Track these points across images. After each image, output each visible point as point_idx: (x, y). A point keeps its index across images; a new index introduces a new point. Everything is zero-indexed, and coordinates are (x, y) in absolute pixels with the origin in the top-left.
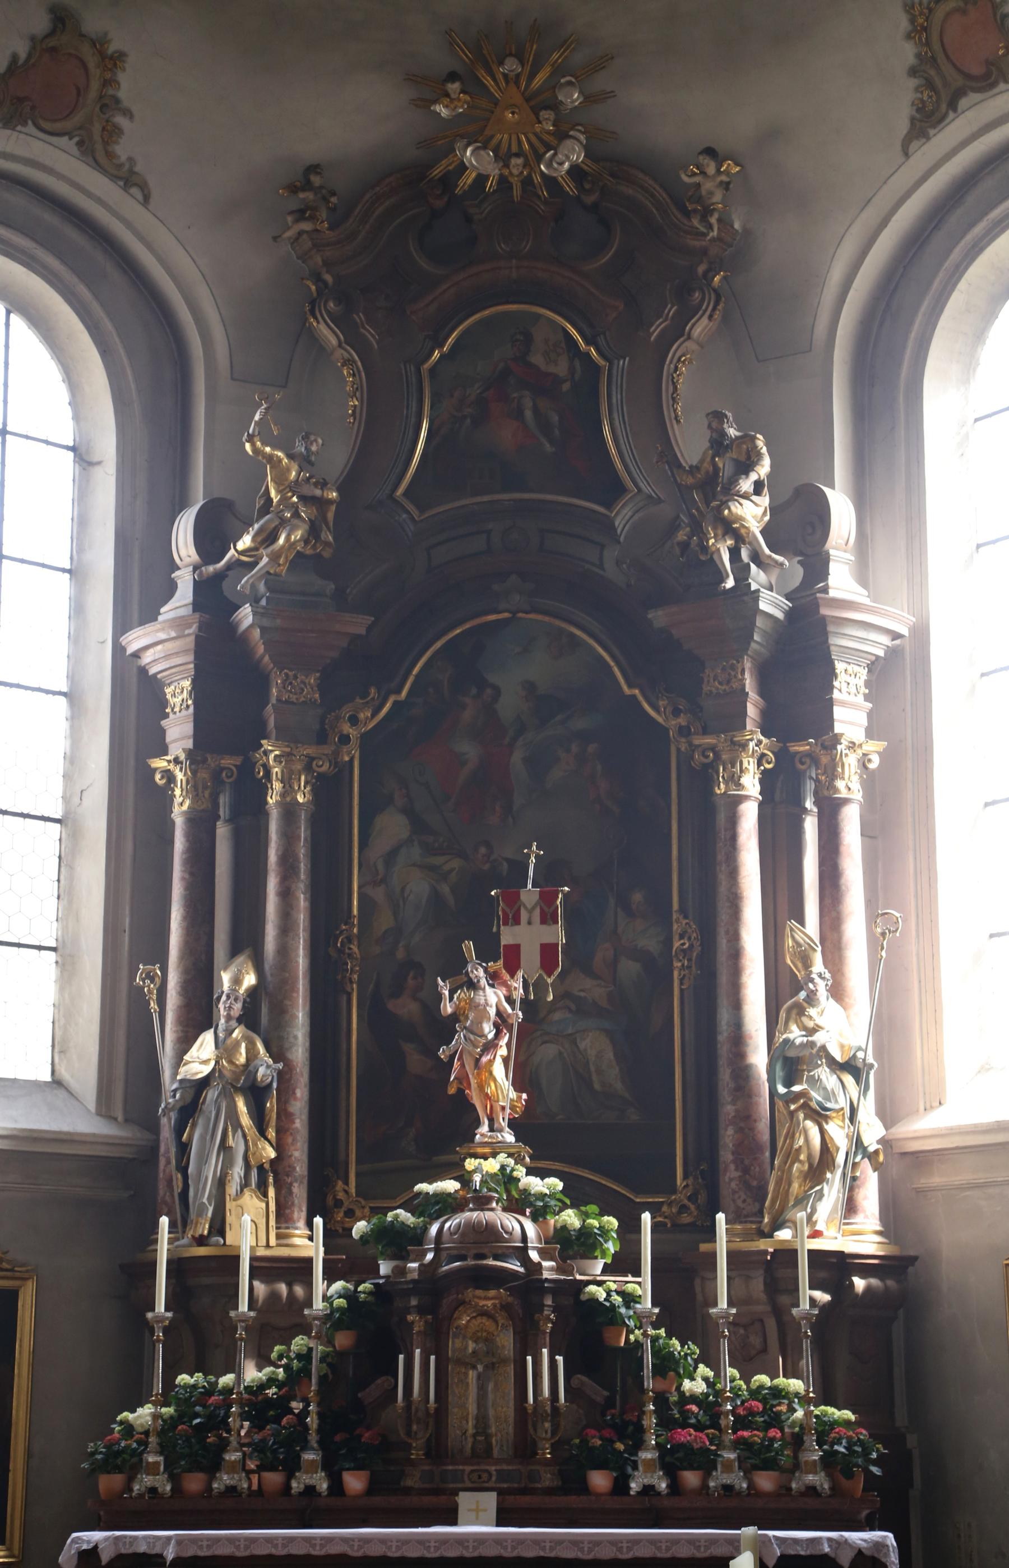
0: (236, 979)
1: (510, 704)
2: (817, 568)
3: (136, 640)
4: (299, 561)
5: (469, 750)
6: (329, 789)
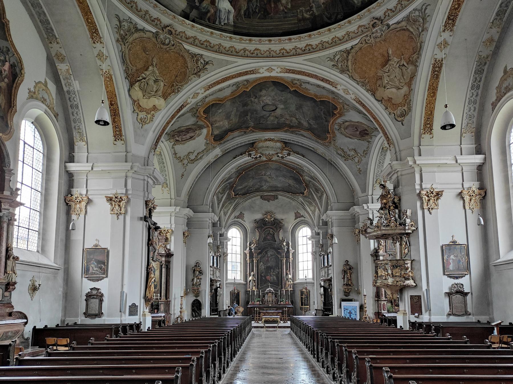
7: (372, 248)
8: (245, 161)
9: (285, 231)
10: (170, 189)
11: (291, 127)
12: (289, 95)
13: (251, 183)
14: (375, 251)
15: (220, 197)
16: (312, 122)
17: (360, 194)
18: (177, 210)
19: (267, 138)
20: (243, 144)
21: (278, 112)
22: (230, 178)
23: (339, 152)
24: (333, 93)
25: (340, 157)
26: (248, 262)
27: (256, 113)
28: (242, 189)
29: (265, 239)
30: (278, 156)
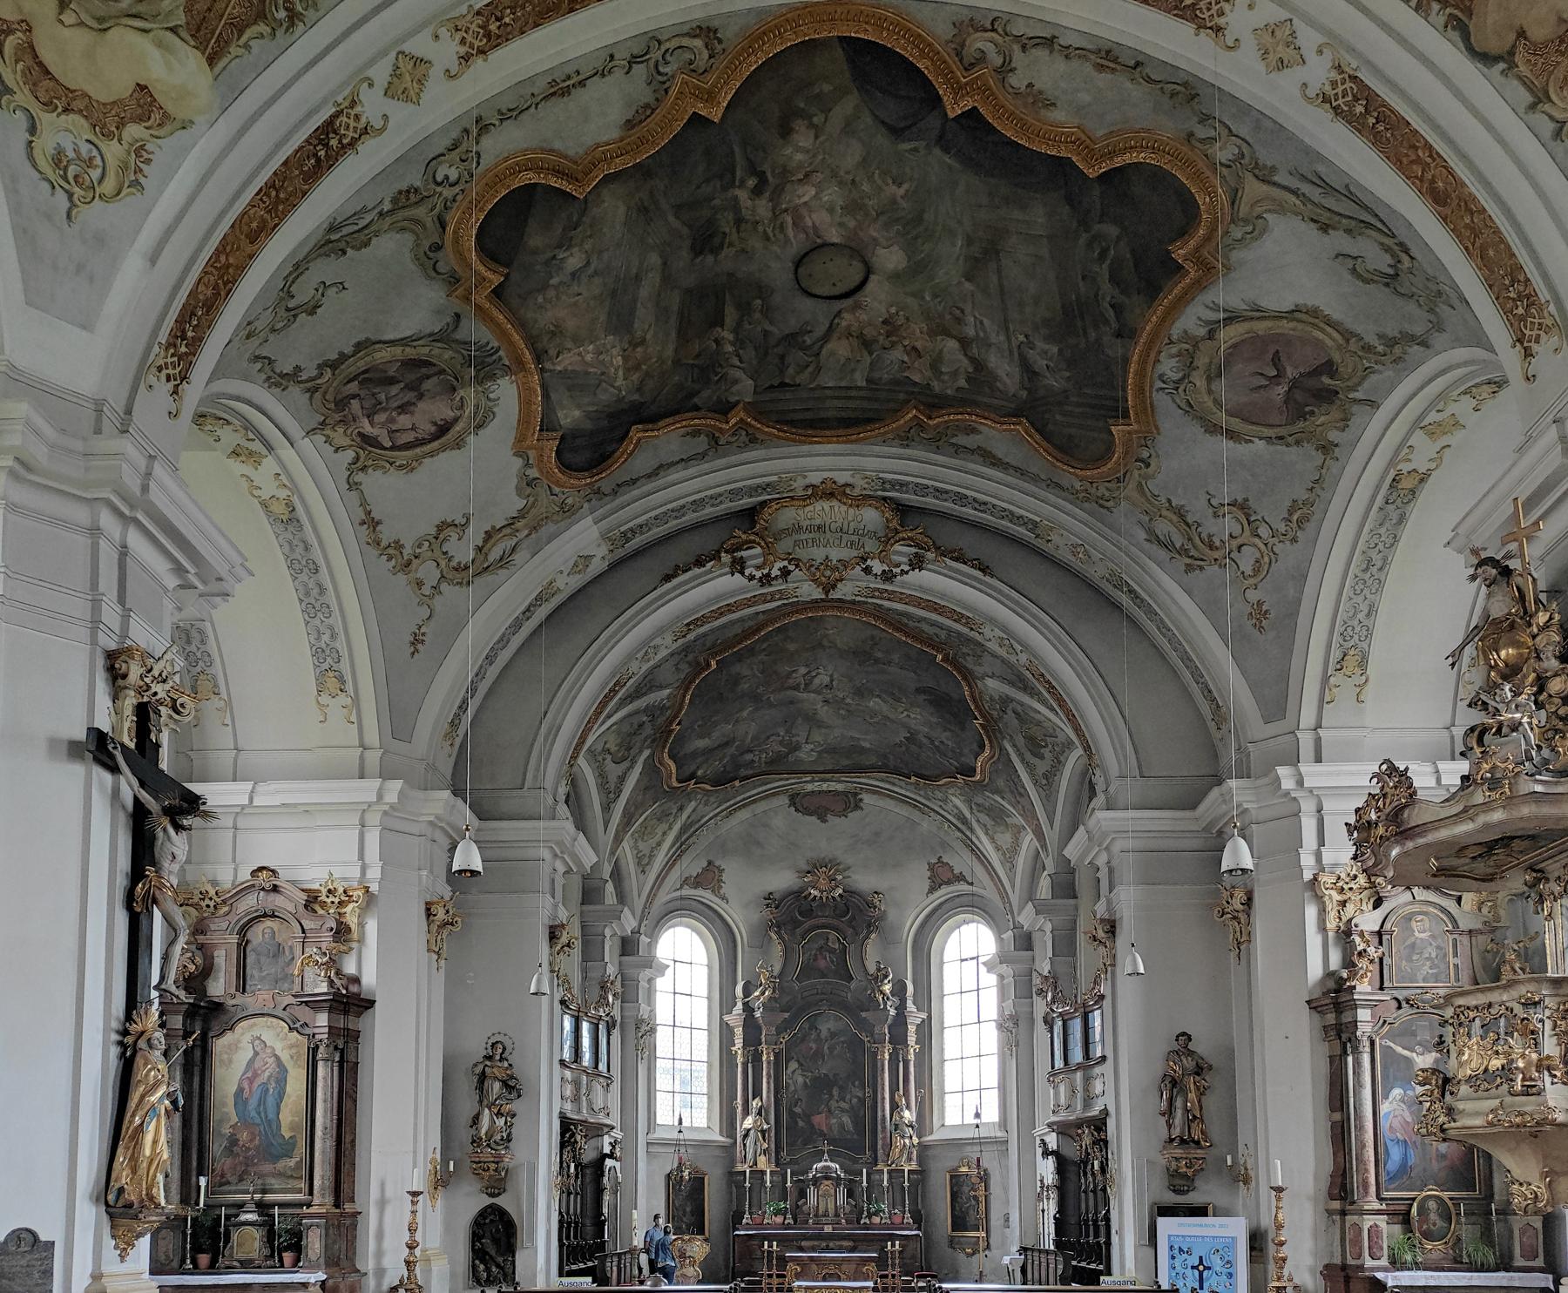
0: (755, 1104)
1: (824, 1033)
2: (903, 1001)
3: (726, 1018)
4: (770, 999)
5: (814, 1046)
6: (777, 1055)
7: (1315, 971)
8: (720, 597)
9: (889, 941)
10: (356, 700)
11: (935, 404)
12: (938, 163)
13: (746, 725)
14: (1331, 984)
15: (613, 779)
16: (1044, 353)
17: (1256, 727)
18: (391, 797)
19: (815, 478)
20: (708, 511)
21: (878, 299)
22: (648, 684)
23: (1163, 527)
24: (1185, 92)
25: (1163, 554)
26: (740, 1060)
27: (767, 311)
28: (708, 752)
29: (807, 971)
30: (868, 570)
